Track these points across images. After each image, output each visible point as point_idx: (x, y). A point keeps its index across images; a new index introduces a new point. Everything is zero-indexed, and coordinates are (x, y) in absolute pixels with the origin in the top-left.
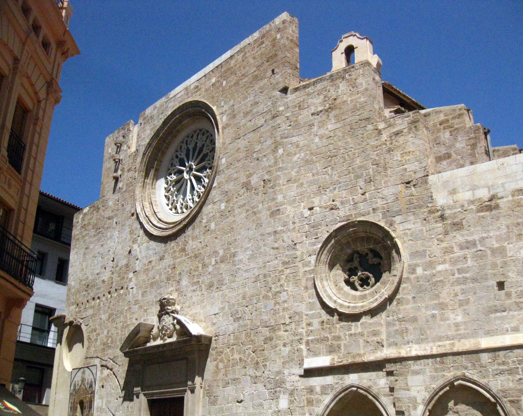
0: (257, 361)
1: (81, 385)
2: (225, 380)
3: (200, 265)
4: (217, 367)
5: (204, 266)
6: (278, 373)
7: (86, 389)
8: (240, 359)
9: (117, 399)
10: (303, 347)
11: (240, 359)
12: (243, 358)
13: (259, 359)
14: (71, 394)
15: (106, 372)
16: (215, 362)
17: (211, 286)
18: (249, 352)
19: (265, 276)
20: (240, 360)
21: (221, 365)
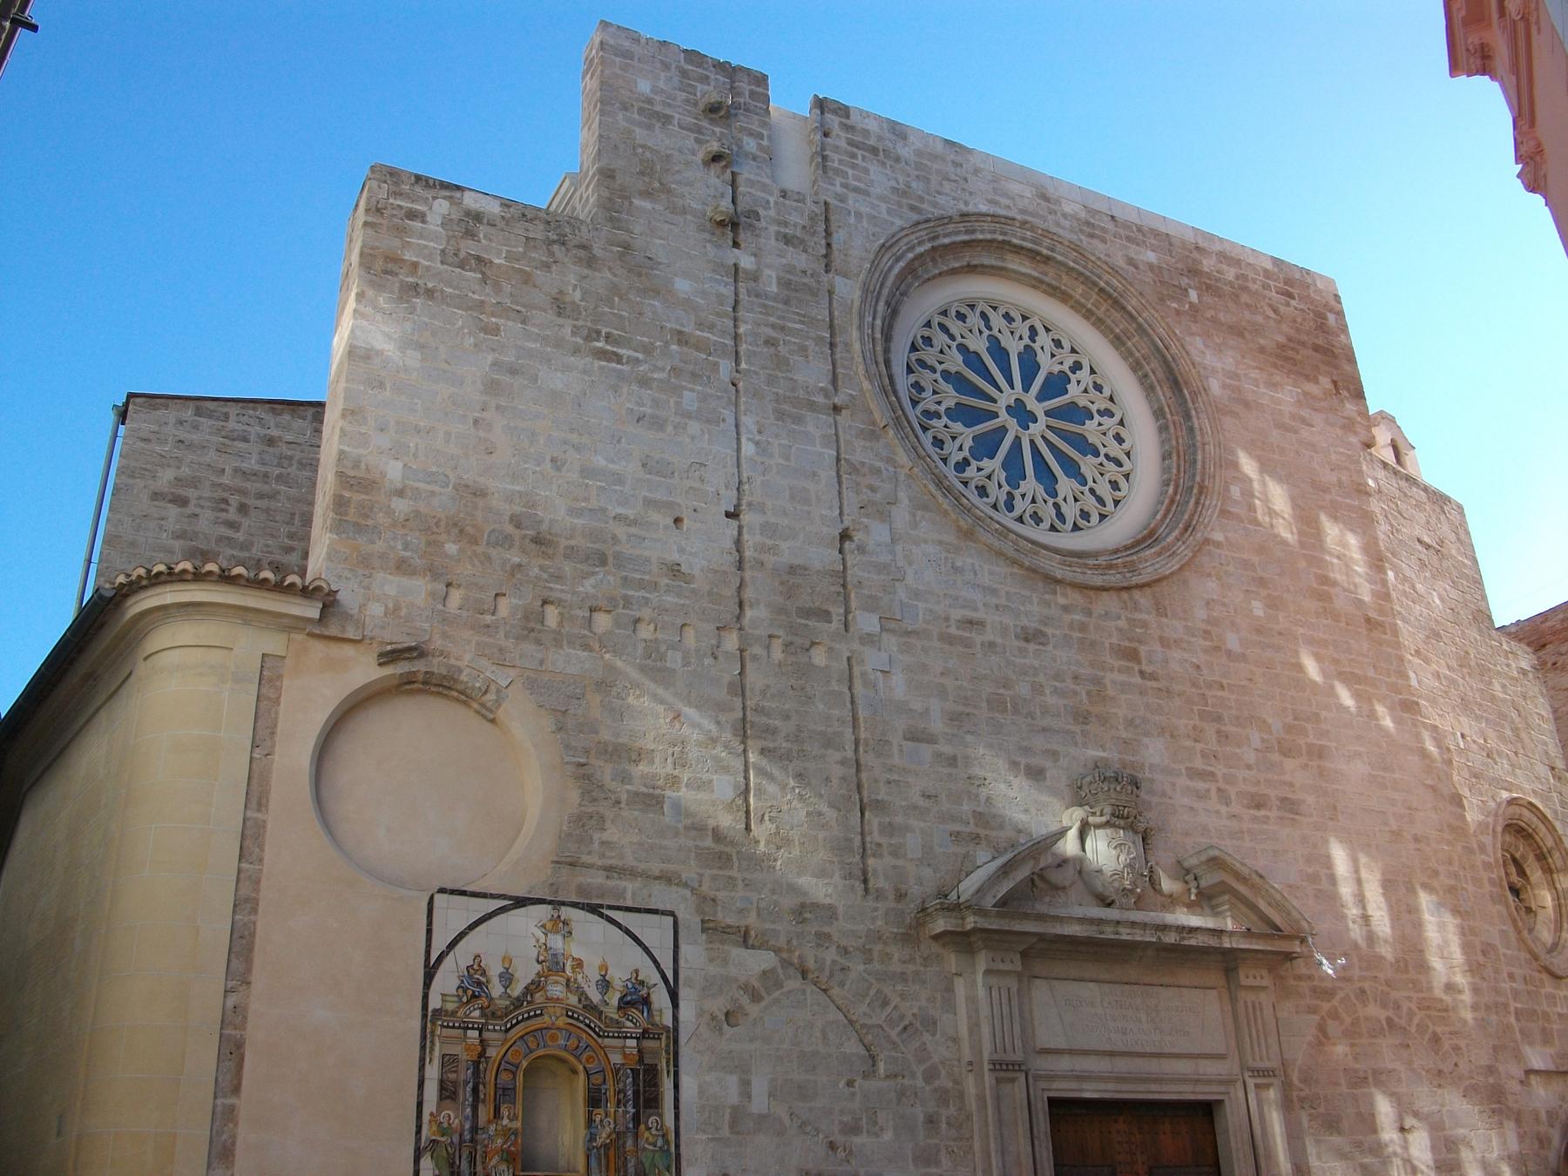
0: (1435, 1034)
1: (535, 986)
2: (1356, 1071)
3: (1210, 730)
4: (1322, 1029)
5: (1223, 736)
6: (1491, 1070)
7: (590, 1007)
8: (1389, 1021)
9: (850, 1084)
10: (1512, 1020)
11: (1389, 1021)
12: (1396, 1019)
13: (1439, 1030)
14: (430, 1018)
15: (756, 962)
16: (1317, 1018)
17: (1258, 803)
18: (1410, 1009)
19: (1416, 839)
20: (1388, 1023)
21: (1332, 1027)
